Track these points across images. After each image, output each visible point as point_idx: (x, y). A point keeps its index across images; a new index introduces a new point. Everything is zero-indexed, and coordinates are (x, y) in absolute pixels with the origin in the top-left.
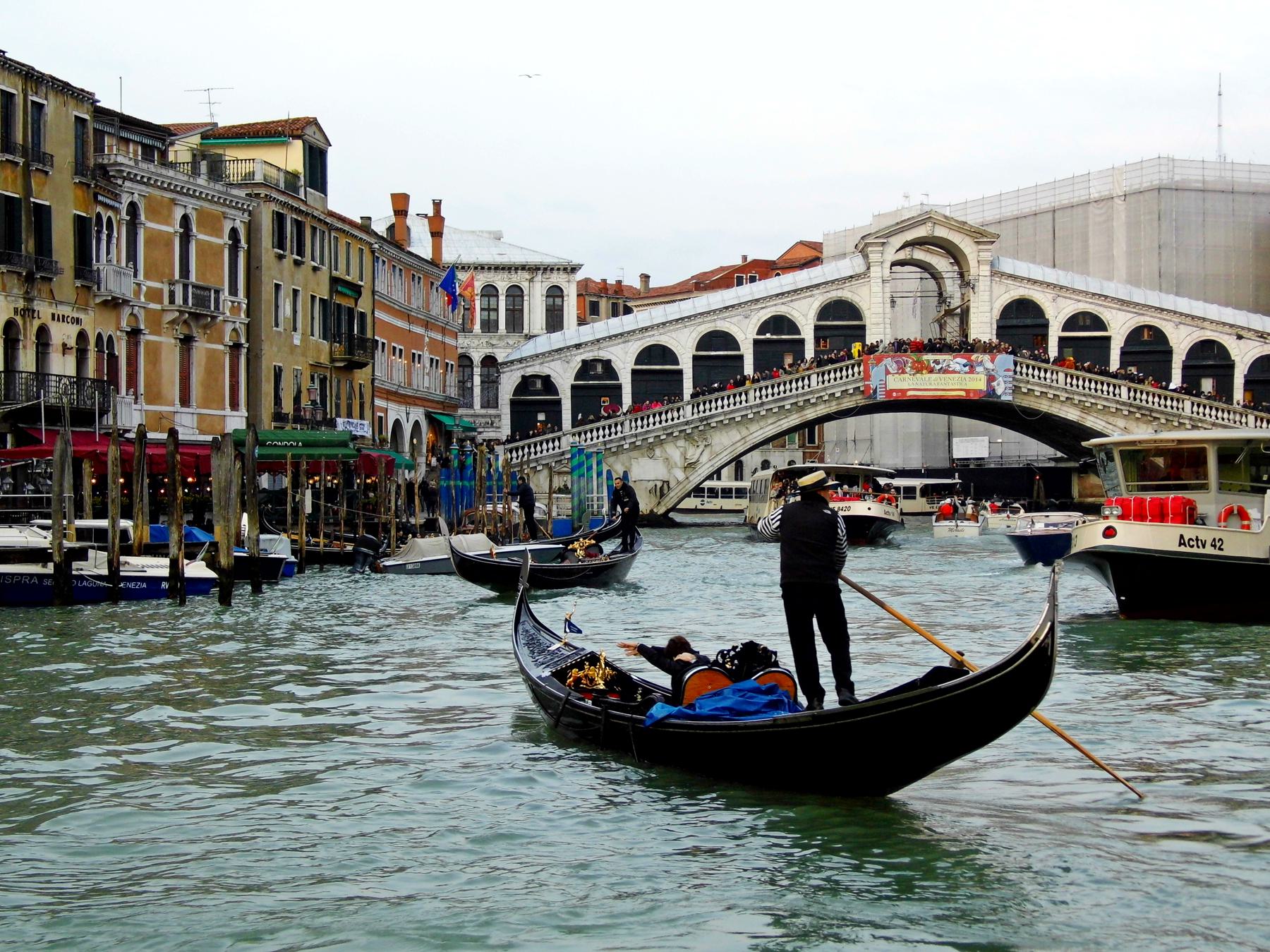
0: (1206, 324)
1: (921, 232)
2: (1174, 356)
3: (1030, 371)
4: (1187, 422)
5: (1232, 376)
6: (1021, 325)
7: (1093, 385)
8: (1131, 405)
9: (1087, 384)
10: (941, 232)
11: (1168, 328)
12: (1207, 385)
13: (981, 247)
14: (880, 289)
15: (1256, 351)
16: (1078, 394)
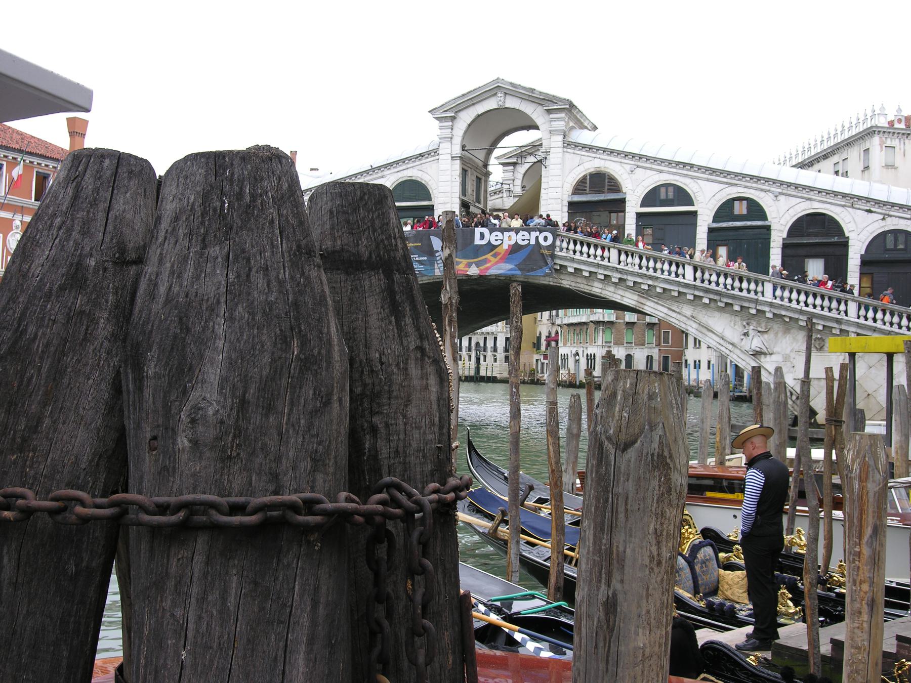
0: (811, 195)
1: (491, 104)
2: (773, 233)
3: (578, 247)
4: (767, 309)
5: (847, 255)
6: (596, 202)
7: (651, 264)
8: (695, 287)
9: (644, 262)
10: (511, 103)
11: (765, 201)
12: (815, 269)
13: (552, 116)
14: (449, 166)
15: (876, 225)
16: (632, 273)
